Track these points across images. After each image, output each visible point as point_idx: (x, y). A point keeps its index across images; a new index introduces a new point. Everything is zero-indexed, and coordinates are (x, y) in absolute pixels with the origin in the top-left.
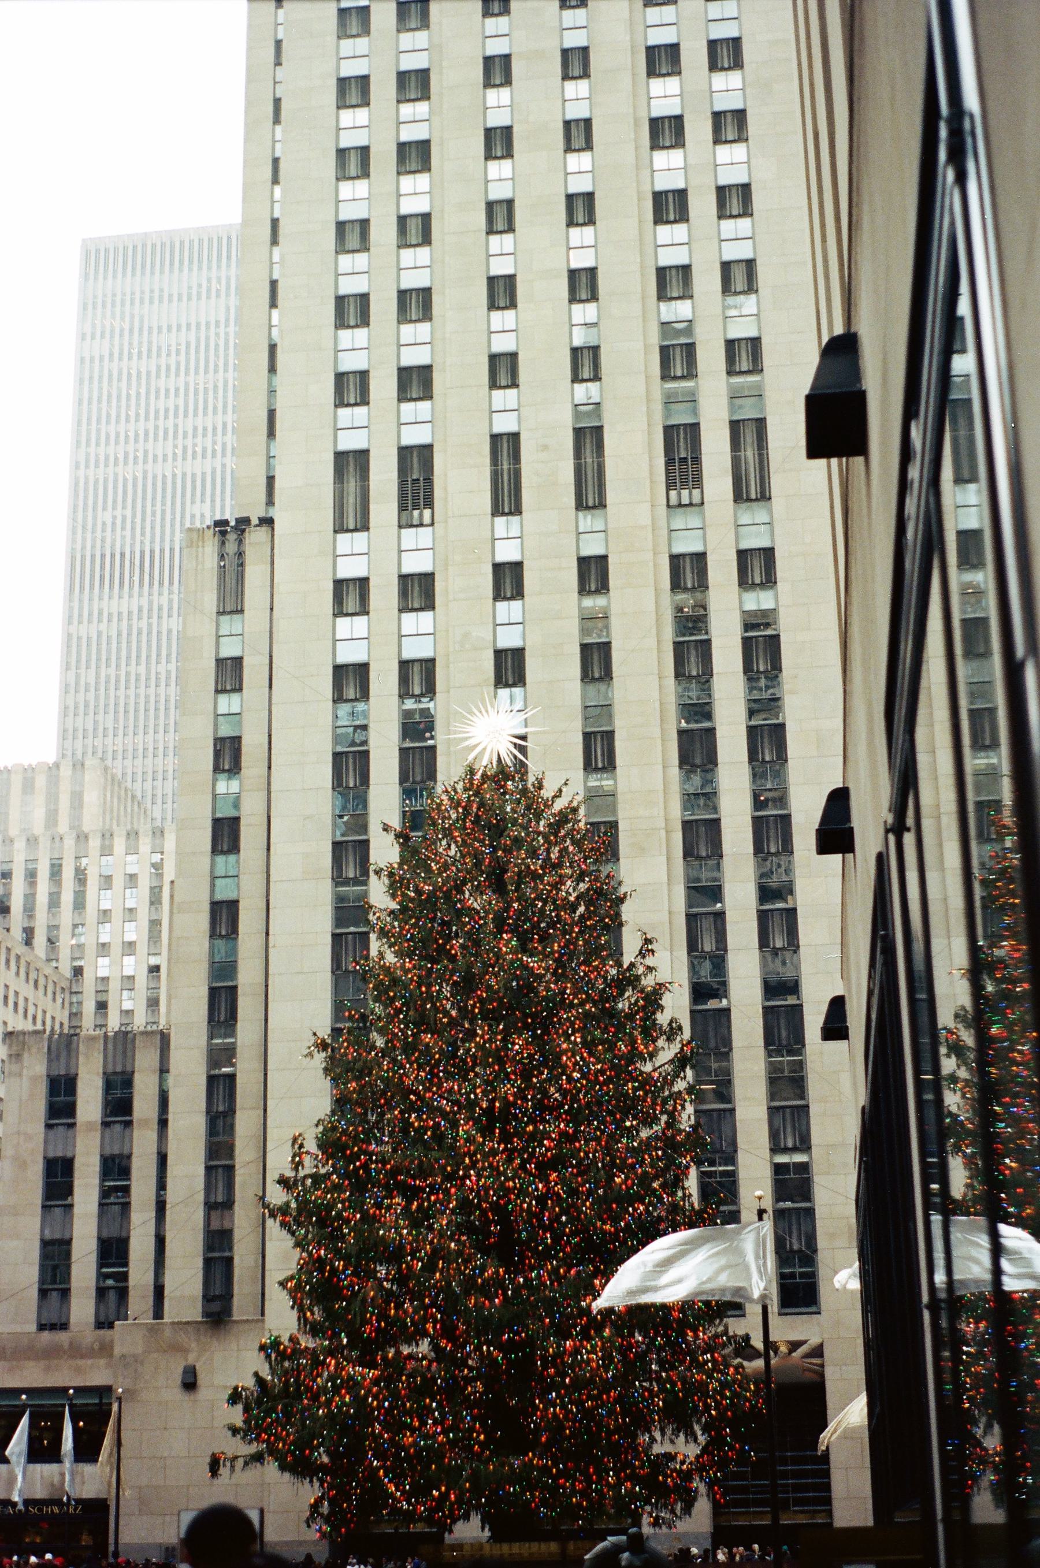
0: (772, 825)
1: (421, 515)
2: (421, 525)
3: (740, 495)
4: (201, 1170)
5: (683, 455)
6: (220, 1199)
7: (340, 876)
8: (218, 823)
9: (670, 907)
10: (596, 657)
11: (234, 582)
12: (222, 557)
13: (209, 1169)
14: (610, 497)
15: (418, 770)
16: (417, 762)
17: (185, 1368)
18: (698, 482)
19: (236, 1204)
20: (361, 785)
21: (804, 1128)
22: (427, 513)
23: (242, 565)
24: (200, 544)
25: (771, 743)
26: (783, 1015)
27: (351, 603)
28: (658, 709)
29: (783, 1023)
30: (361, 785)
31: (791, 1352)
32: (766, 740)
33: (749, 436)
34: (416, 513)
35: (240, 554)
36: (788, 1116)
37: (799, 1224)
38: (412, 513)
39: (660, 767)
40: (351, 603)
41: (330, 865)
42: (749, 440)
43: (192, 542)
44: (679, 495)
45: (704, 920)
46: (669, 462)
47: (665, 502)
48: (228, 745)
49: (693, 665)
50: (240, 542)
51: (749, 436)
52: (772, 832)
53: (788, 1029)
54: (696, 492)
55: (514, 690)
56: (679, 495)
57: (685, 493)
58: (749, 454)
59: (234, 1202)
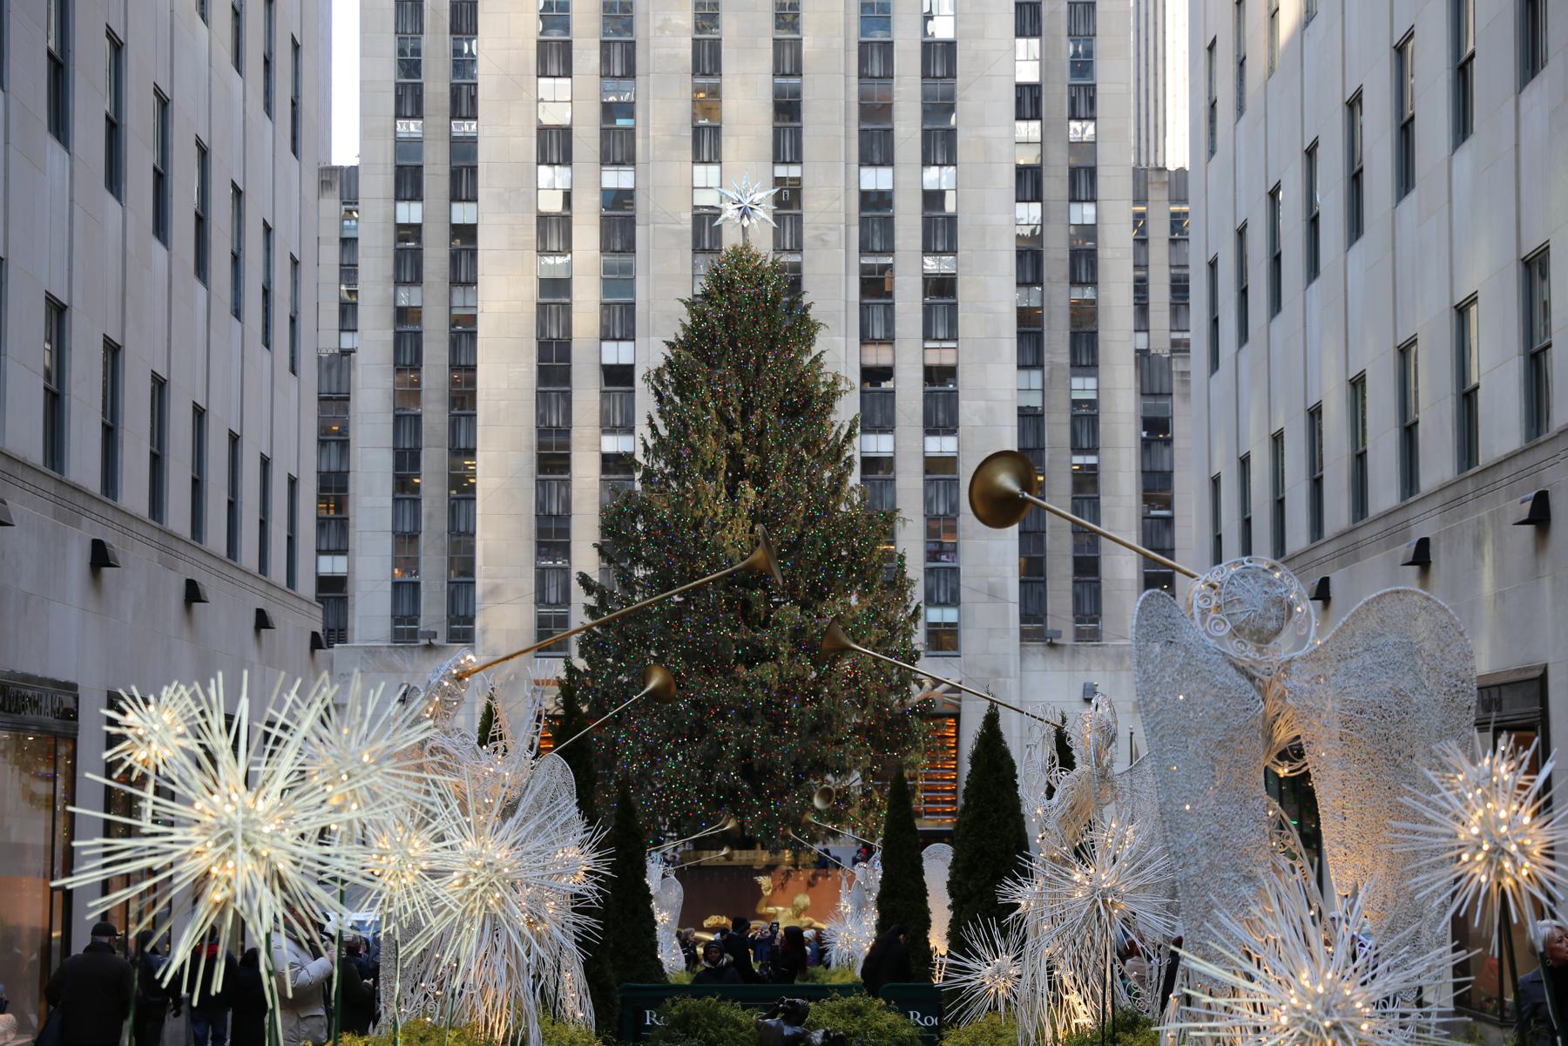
0: (940, 225)
4: (389, 502)
8: (400, 171)
9: (846, 296)
13: (396, 500)
15: (618, 150)
21: (954, 499)
25: (943, 146)
26: (940, 400)
28: (843, 105)
29: (940, 407)
31: (934, 687)
32: (939, 144)
36: (941, 486)
37: (946, 580)
39: (843, 164)
45: (875, 310)
48: (409, 91)
49: (876, 64)
52: (940, 233)
53: (944, 413)
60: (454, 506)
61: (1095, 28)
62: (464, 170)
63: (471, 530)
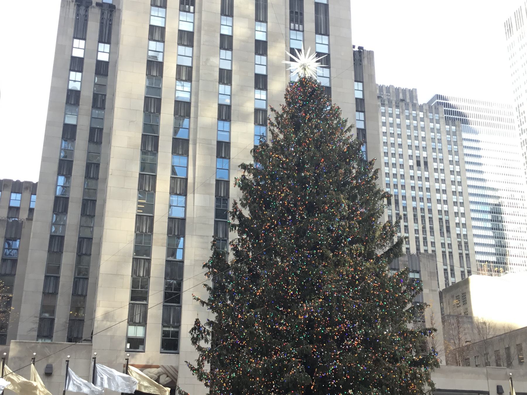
1: (189, 8)
2: (189, 12)
3: (318, 32)
4: (43, 278)
5: (297, 11)
6: (51, 291)
7: (145, 149)
10: (261, 80)
11: (82, 27)
12: (77, 15)
13: (46, 277)
15: (182, 111)
16: (182, 108)
17: (47, 365)
18: (302, 22)
19: (59, 294)
20: (157, 112)
22: (192, 8)
23: (86, 20)
24: (68, 7)
30: (157, 112)
33: (322, 10)
34: (187, 6)
35: (86, 16)
38: (185, 7)
40: (157, 36)
41: (140, 144)
42: (322, 11)
43: (64, 6)
44: (295, 26)
46: (291, 12)
47: (289, 27)
50: (86, 11)
51: (322, 10)
54: (301, 26)
55: (226, 86)
56: (295, 26)
57: (297, 25)
58: (322, 17)
59: (58, 294)
60: (77, 281)
61: (364, 108)
62: (97, 129)
63: (84, 294)
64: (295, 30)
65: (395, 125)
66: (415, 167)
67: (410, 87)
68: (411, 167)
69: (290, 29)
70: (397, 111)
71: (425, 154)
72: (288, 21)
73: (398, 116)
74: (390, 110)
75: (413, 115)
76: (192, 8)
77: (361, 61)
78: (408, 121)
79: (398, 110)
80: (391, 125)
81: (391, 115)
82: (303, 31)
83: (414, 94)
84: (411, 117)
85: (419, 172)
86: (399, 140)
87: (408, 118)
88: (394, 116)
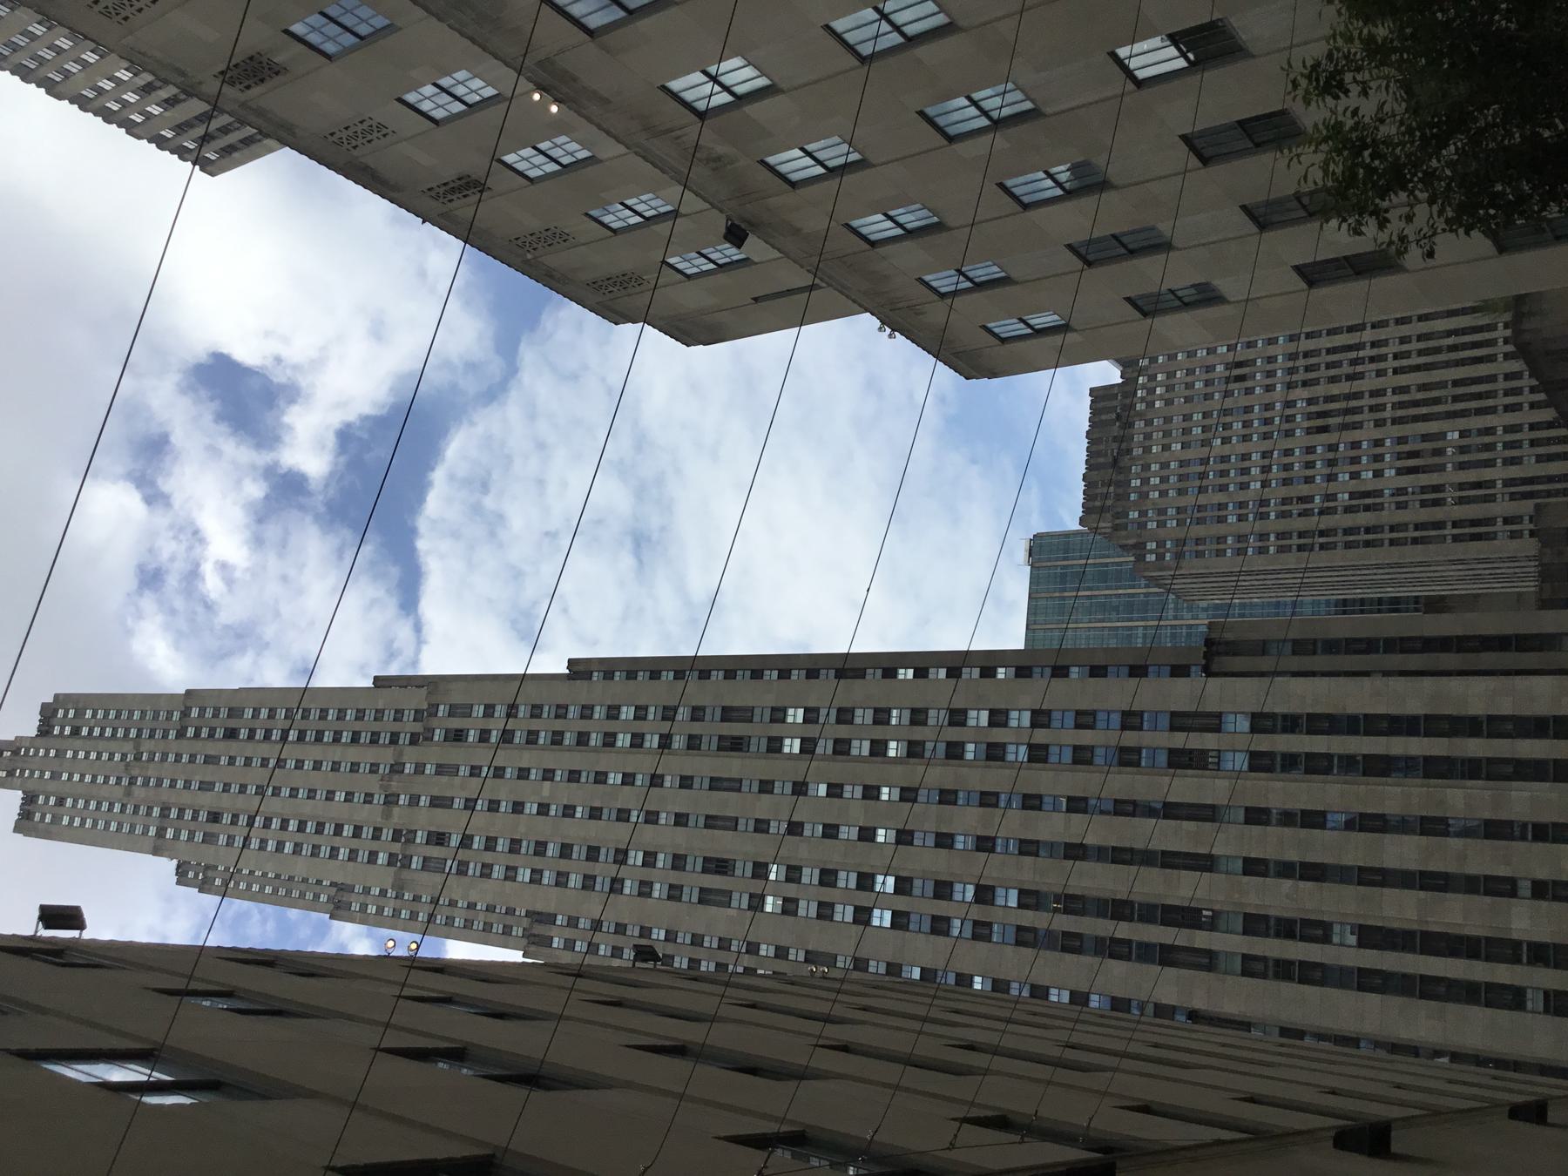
1: (1205, 916)
3: (1218, 729)
14: (1209, 802)
27: (1259, 967)
57: (1210, 760)
64: (1218, 764)
65: (1166, 427)
66: (1249, 384)
67: (1088, 400)
68: (1249, 391)
69: (1218, 770)
70: (1139, 424)
71: (1220, 368)
72: (1207, 772)
73: (1149, 423)
74: (1138, 438)
75: (1144, 395)
76: (1205, 913)
77: (1227, 643)
78: (1158, 404)
79: (1137, 423)
80: (1167, 434)
81: (1148, 436)
82: (1219, 751)
83: (1101, 393)
84: (1149, 398)
85: (1258, 376)
86: (1197, 417)
87: (1151, 404)
88: (1149, 429)
